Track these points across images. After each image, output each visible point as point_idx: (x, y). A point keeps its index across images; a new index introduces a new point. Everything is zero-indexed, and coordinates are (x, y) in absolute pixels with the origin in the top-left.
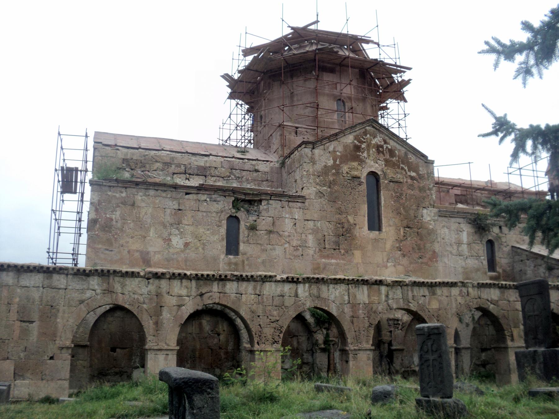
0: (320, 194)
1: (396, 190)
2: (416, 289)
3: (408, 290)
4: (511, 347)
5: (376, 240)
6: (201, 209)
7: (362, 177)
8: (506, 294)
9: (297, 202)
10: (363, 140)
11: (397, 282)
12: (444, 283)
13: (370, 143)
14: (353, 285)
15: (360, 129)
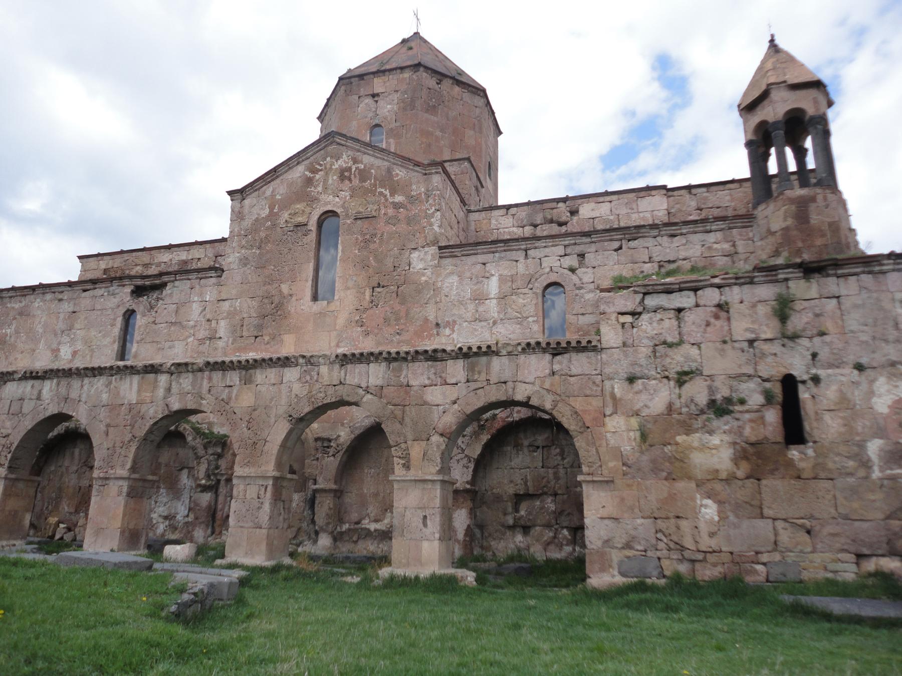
0: (244, 261)
1: (366, 231)
2: (217, 376)
3: (203, 378)
4: (398, 481)
5: (322, 314)
6: (98, 307)
7: (311, 223)
8: (404, 373)
9: (211, 277)
10: (318, 167)
11: (179, 365)
12: (264, 360)
13: (331, 168)
14: (118, 377)
15: (315, 153)
